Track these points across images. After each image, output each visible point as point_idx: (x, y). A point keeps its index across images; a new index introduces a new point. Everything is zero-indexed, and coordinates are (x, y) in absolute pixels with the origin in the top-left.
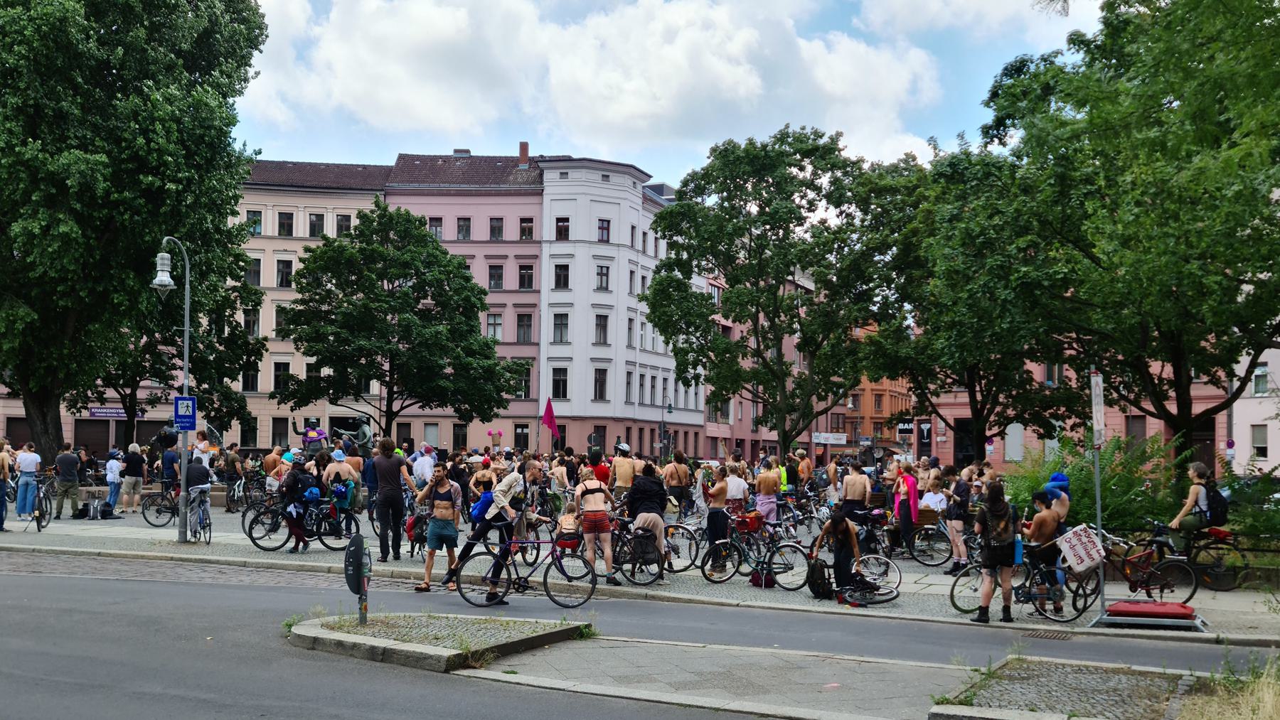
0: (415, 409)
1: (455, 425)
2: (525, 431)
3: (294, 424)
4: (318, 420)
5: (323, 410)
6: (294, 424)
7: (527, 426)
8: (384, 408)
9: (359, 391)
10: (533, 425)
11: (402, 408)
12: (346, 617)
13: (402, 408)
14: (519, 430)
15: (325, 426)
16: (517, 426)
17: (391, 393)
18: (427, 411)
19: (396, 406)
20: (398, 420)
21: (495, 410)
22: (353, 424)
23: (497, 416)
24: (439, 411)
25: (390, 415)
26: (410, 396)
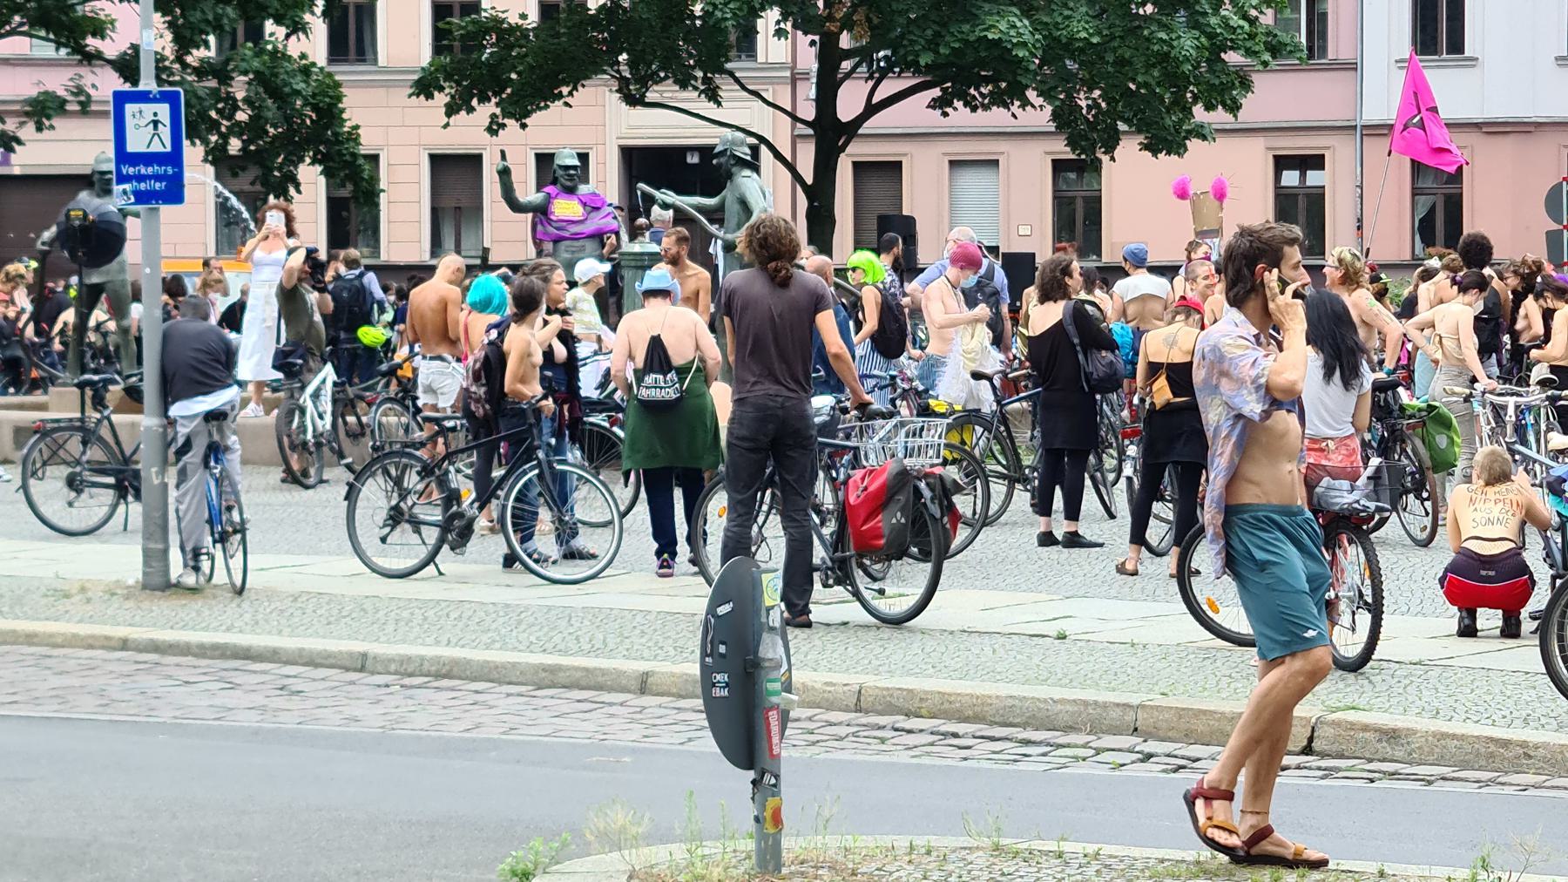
0: (916, 112)
1: (1059, 166)
2: (1314, 178)
3: (505, 173)
4: (583, 157)
5: (596, 122)
6: (505, 173)
7: (1317, 162)
8: (808, 112)
9: (710, 55)
10: (1340, 153)
11: (871, 109)
12: (711, 848)
13: (871, 109)
14: (1290, 178)
15: (606, 180)
16: (1282, 163)
17: (829, 57)
18: (960, 116)
19: (849, 103)
20: (857, 150)
21: (1199, 113)
22: (698, 171)
23: (1200, 133)
24: (997, 117)
25: (830, 134)
26: (901, 63)
